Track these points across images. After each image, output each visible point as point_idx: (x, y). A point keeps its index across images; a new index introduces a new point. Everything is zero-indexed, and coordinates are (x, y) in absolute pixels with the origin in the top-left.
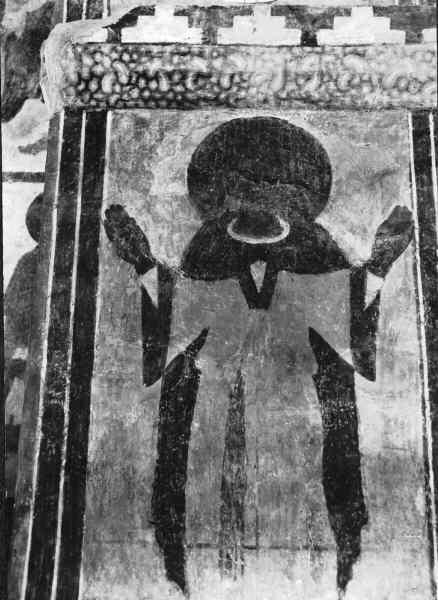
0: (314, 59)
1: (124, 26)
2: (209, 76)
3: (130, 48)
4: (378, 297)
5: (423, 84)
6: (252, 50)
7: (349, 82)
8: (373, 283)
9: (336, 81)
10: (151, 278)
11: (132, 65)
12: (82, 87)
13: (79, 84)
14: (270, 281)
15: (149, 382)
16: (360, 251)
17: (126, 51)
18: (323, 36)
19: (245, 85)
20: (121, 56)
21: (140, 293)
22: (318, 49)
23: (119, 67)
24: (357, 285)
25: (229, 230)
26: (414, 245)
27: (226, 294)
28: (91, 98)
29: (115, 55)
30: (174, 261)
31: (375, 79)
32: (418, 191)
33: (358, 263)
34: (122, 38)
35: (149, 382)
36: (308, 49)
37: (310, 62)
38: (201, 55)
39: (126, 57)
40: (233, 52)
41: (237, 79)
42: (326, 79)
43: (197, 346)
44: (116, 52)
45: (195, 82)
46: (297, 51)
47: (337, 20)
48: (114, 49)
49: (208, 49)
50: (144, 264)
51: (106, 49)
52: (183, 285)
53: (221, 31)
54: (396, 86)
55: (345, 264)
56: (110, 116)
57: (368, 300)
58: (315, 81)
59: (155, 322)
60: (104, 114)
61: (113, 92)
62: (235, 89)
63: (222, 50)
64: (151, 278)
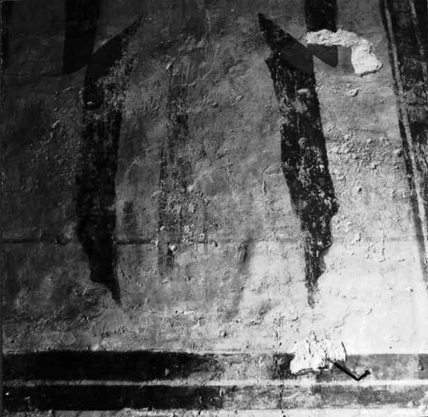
35: (69, 67)
43: (130, 31)
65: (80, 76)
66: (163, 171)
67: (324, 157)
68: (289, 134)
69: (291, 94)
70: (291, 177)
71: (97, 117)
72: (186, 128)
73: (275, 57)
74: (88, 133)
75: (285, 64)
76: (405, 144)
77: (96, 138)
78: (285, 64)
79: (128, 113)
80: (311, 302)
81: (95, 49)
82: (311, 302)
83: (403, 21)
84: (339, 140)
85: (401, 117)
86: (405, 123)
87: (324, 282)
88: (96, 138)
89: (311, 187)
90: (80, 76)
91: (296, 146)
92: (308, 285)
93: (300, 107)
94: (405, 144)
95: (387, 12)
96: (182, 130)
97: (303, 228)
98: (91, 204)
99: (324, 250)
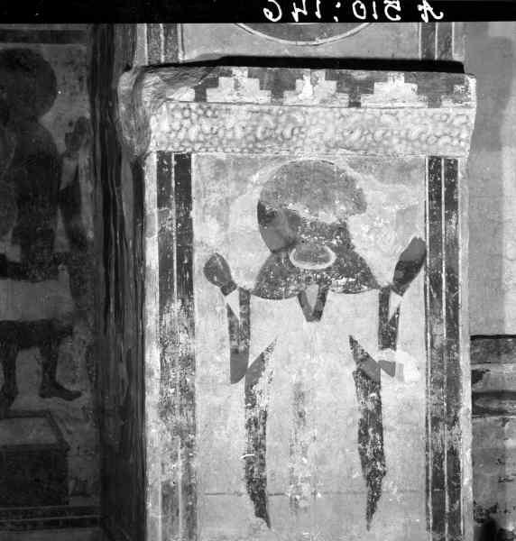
0: (357, 117)
1: (208, 87)
2: (275, 129)
3: (214, 106)
4: (398, 309)
5: (439, 137)
6: (310, 110)
7: (383, 134)
8: (395, 299)
9: (373, 134)
10: (233, 299)
11: (215, 120)
12: (173, 135)
13: (170, 133)
14: (322, 298)
15: (235, 379)
16: (386, 276)
17: (209, 108)
18: (366, 100)
19: (303, 136)
20: (205, 113)
21: (226, 311)
22: (362, 110)
23: (203, 120)
24: (384, 300)
25: (291, 258)
26: (425, 270)
27: (289, 308)
28: (181, 146)
29: (200, 112)
30: (250, 284)
31: (403, 134)
32: (430, 225)
33: (386, 284)
34: (208, 98)
35: (235, 379)
36: (353, 109)
37: (355, 115)
38: (269, 112)
39: (209, 113)
40: (295, 110)
41: (296, 131)
42: (365, 133)
44: (202, 109)
45: (264, 133)
46: (345, 111)
47: (376, 85)
48: (200, 107)
49: (275, 109)
50: (227, 287)
51: (194, 106)
52: (255, 301)
53: (286, 93)
54: (419, 139)
55: (376, 286)
56: (193, 156)
57: (392, 312)
58: (357, 134)
59: (240, 330)
60: (189, 155)
61: (198, 142)
62: (294, 139)
63: (286, 108)
64: (233, 299)
65: (241, 385)
66: (291, 450)
67: (382, 440)
68: (364, 425)
69: (366, 395)
70: (362, 453)
71: (253, 414)
72: (304, 420)
73: (359, 370)
74: (248, 426)
75: (364, 375)
76: (427, 431)
77: (253, 428)
78: (364, 375)
79: (270, 411)
80: (368, 528)
81: (249, 365)
82: (368, 528)
83: (437, 343)
84: (392, 429)
85: (427, 414)
86: (429, 418)
87: (376, 516)
88: (253, 428)
89: (374, 460)
90: (241, 385)
91: (367, 434)
92: (368, 518)
93: (371, 406)
94: (427, 431)
95: (428, 334)
96: (302, 422)
97: (367, 485)
98: (252, 471)
99: (377, 498)
